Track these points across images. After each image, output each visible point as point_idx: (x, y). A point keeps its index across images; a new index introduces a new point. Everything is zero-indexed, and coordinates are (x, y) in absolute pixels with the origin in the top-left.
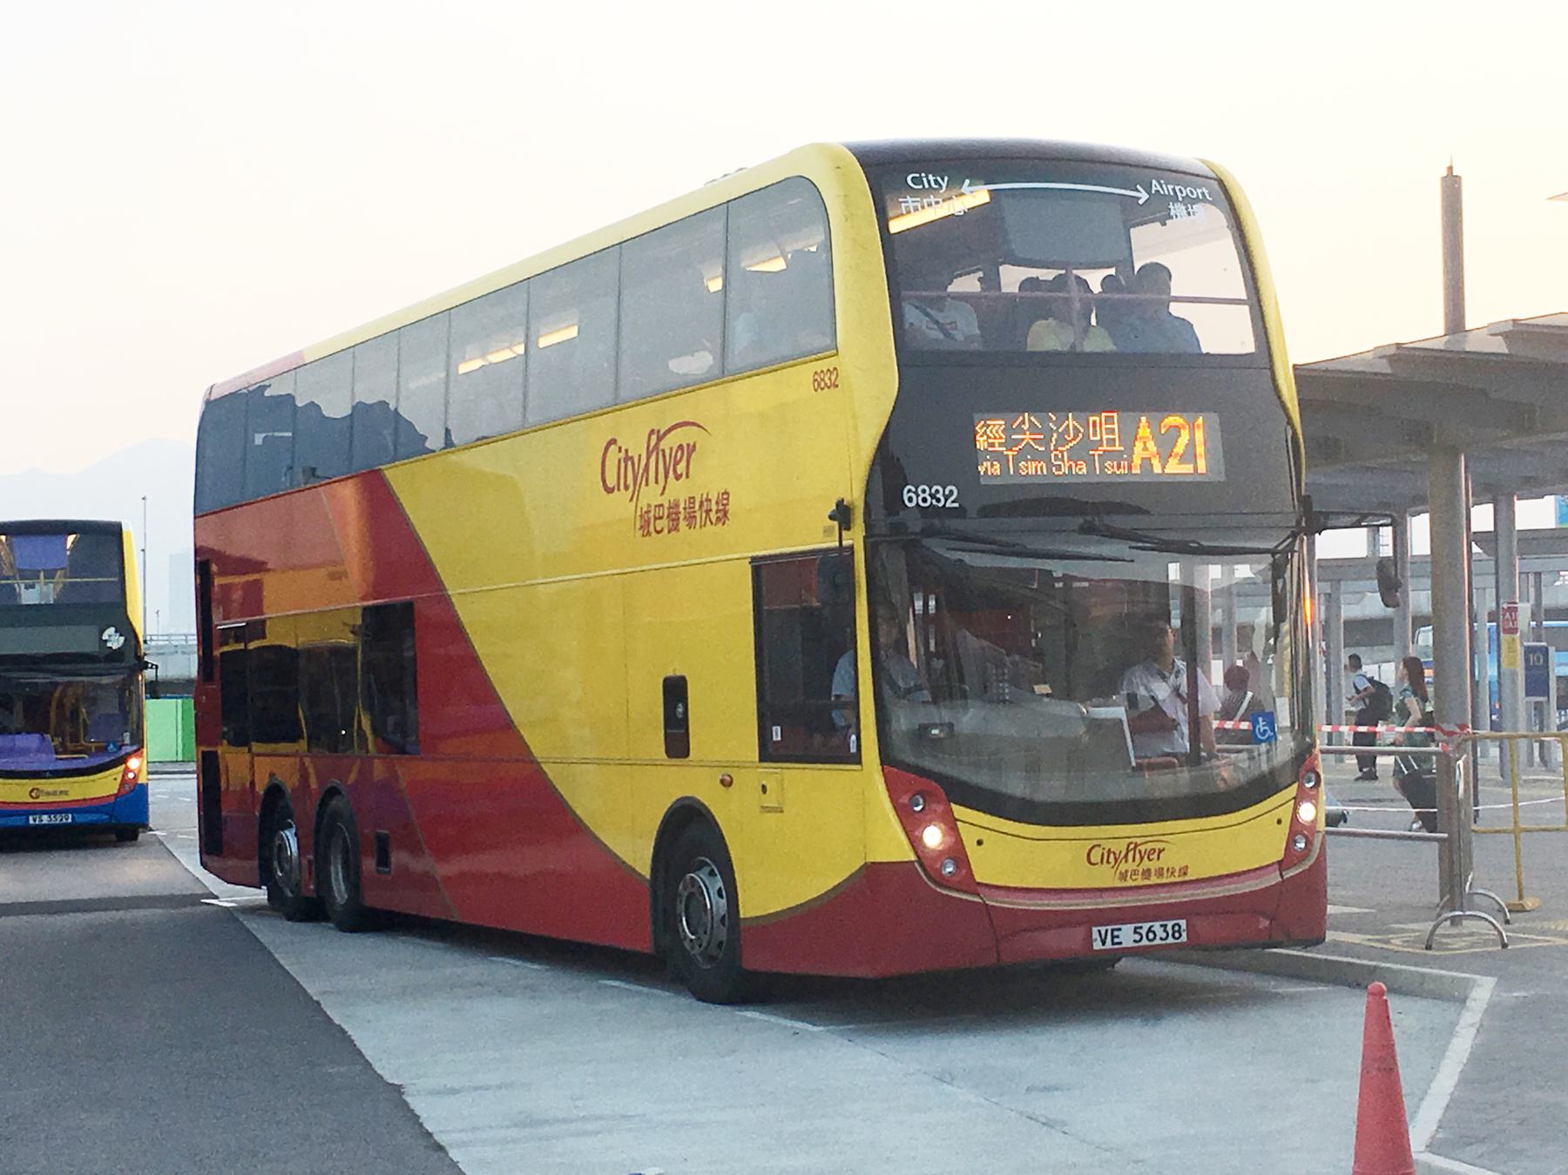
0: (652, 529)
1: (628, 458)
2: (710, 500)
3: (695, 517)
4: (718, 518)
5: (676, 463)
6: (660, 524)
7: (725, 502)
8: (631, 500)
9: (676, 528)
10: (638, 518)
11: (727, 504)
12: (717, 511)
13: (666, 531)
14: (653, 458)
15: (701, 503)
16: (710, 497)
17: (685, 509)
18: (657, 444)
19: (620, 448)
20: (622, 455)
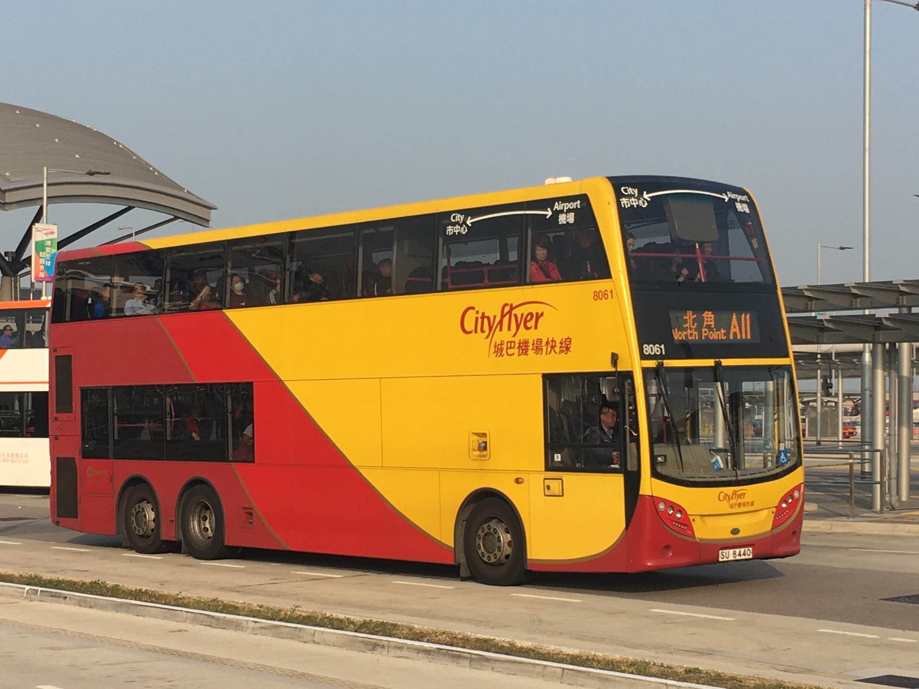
0: (504, 352)
1: (483, 317)
2: (555, 342)
3: (542, 349)
4: (560, 351)
5: (526, 321)
6: (510, 351)
7: (567, 343)
8: (487, 337)
9: (526, 354)
10: (493, 349)
11: (570, 344)
12: (561, 347)
13: (516, 354)
14: (506, 319)
15: (547, 343)
16: (554, 340)
17: (533, 344)
18: (510, 312)
19: (477, 312)
20: (480, 315)
